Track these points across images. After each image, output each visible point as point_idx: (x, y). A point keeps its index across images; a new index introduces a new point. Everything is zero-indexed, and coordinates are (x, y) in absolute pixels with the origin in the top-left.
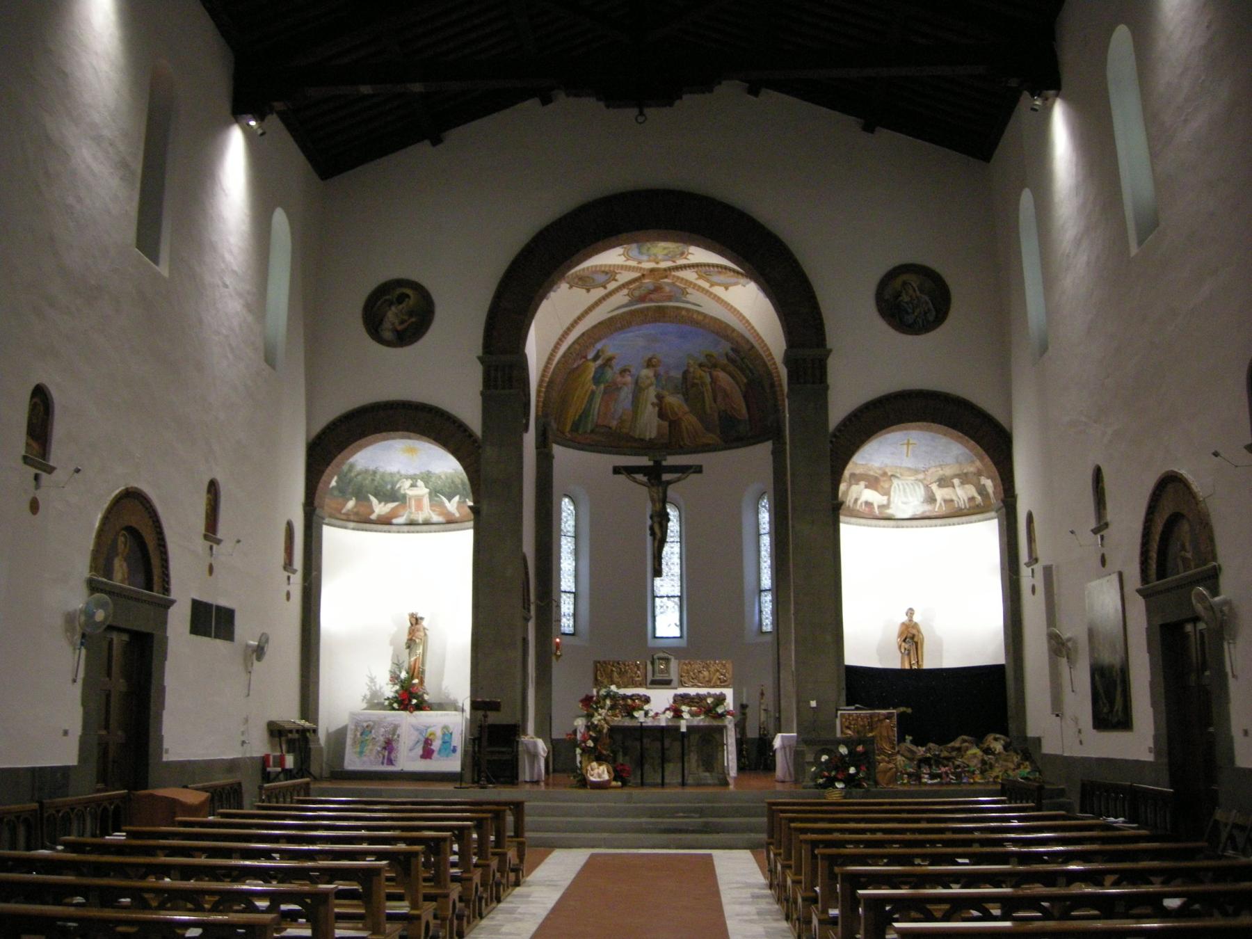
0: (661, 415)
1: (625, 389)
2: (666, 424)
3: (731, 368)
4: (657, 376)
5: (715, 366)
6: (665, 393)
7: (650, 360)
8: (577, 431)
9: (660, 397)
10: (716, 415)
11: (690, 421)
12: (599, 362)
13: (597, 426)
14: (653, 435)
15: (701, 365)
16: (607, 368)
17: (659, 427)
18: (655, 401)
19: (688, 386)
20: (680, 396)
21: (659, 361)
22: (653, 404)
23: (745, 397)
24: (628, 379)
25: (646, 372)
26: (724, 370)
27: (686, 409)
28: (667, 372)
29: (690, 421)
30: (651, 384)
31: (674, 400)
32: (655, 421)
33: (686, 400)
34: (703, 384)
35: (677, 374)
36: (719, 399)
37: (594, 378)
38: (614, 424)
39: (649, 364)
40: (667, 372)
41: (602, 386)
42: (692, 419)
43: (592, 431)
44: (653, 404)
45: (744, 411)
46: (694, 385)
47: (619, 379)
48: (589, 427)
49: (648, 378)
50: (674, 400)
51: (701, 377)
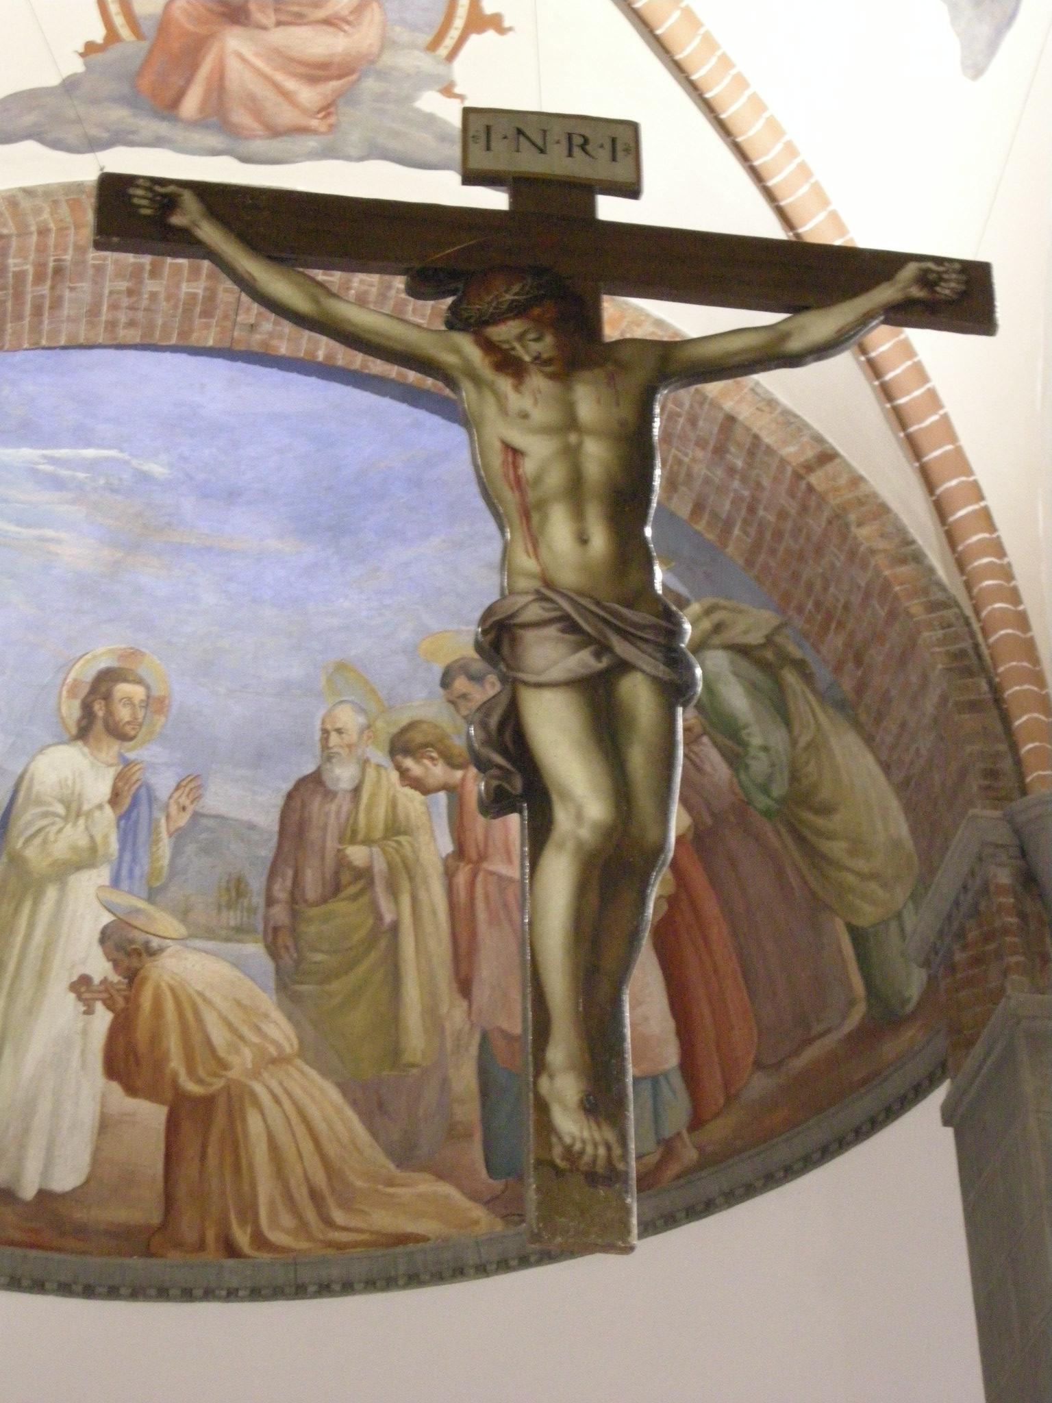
0: (126, 1061)
2: (152, 1114)
4: (128, 799)
6: (165, 924)
7: (105, 681)
9: (128, 950)
10: (465, 1078)
11: (299, 1107)
14: (66, 1179)
15: (402, 746)
17: (105, 1125)
18: (100, 968)
19: (305, 891)
20: (254, 950)
21: (155, 704)
22: (81, 986)
25: (73, 771)
27: (280, 1030)
28: (191, 784)
29: (299, 1107)
30: (87, 859)
31: (216, 978)
32: (88, 1090)
33: (289, 981)
34: (403, 872)
35: (249, 804)
39: (98, 712)
40: (191, 784)
42: (324, 1099)
44: (81, 986)
46: (346, 880)
49: (74, 809)
50: (216, 978)
51: (396, 828)
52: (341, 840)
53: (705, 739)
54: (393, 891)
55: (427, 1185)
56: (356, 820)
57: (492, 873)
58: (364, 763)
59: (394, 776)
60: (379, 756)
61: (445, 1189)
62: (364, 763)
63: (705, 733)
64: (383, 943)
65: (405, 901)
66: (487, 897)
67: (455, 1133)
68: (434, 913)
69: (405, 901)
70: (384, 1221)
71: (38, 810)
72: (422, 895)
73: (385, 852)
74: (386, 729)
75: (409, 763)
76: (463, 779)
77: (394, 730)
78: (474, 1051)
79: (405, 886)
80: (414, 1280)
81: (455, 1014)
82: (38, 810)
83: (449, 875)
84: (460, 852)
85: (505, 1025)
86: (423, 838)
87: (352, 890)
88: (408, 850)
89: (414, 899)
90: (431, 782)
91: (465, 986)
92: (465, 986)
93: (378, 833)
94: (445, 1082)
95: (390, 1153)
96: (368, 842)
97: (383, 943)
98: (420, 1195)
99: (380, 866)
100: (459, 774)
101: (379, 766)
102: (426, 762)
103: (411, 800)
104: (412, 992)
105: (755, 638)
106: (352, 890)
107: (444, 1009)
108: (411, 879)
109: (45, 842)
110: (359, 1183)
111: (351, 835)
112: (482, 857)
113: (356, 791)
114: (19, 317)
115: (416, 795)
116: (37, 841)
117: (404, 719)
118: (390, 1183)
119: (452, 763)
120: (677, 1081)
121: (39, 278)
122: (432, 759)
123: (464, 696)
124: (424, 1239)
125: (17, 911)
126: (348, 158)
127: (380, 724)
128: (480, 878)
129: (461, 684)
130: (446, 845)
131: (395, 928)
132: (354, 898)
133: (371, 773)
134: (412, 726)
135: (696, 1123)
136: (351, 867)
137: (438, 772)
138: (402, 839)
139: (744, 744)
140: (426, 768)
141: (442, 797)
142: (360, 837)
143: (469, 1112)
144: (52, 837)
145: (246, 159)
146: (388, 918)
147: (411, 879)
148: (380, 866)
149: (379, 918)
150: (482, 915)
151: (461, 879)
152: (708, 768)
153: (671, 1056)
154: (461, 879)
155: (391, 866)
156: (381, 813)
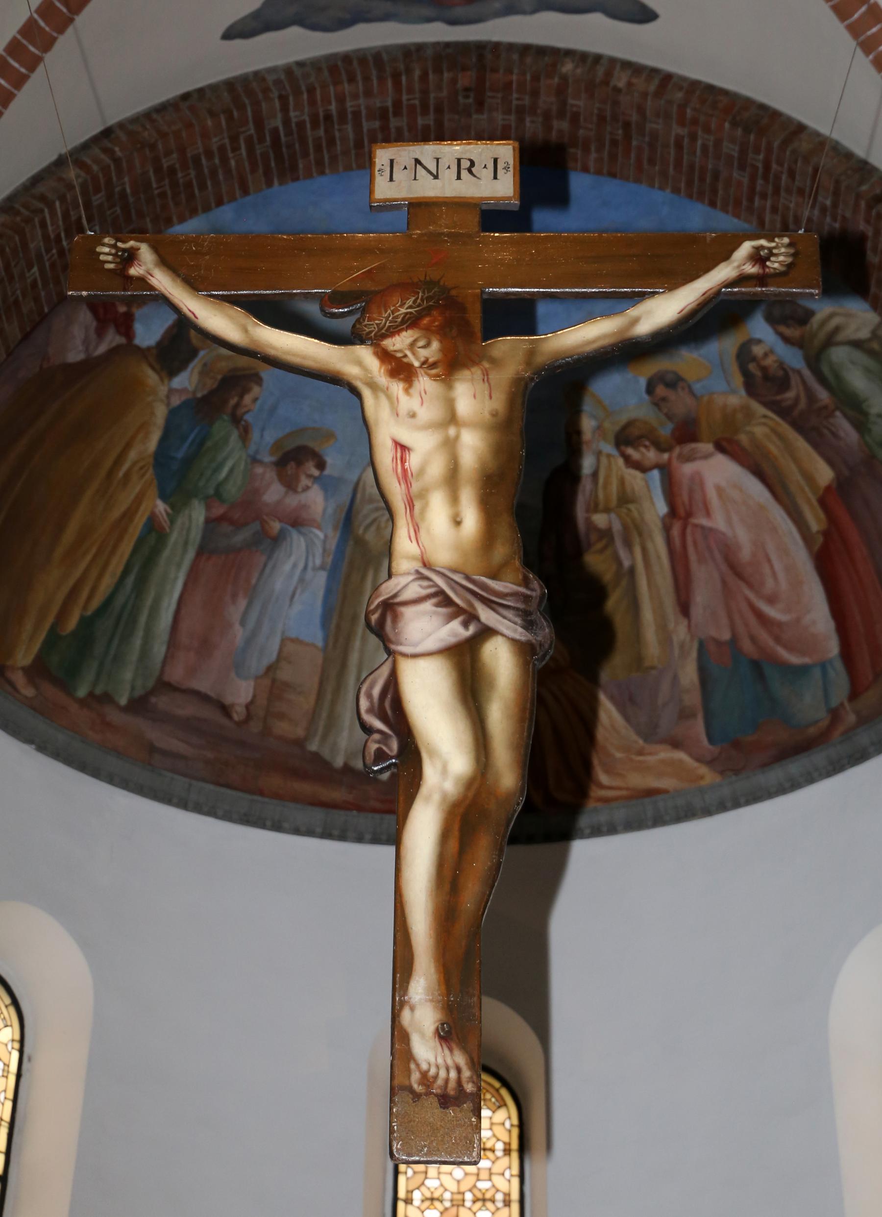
1: (297, 542)
3: (763, 427)
5: (687, 433)
8: (65, 684)
10: (689, 674)
12: (186, 381)
13: (164, 686)
16: (222, 427)
23: (827, 561)
24: (315, 500)
26: (725, 446)
34: (634, 530)
36: (703, 595)
37: (161, 458)
38: (241, 693)
41: (198, 514)
43: (139, 705)
45: (819, 618)
47: (273, 492)
48: (127, 683)
51: (626, 499)
52: (588, 511)
53: (838, 413)
54: (628, 544)
55: (665, 754)
56: (596, 496)
57: (696, 526)
58: (599, 454)
59: (621, 461)
60: (608, 448)
61: (681, 755)
62: (599, 454)
63: (837, 408)
64: (624, 582)
65: (638, 551)
66: (695, 543)
67: (685, 715)
68: (659, 557)
69: (638, 551)
70: (638, 781)
71: (371, 506)
72: (649, 545)
73: (620, 517)
74: (612, 427)
75: (630, 451)
76: (670, 459)
77: (617, 428)
78: (694, 654)
79: (636, 540)
80: (658, 821)
81: (680, 631)
82: (371, 506)
83: (667, 529)
84: (673, 512)
85: (713, 633)
86: (646, 505)
87: (599, 546)
88: (635, 514)
89: (644, 551)
90: (647, 463)
91: (684, 608)
92: (684, 608)
93: (614, 502)
94: (675, 679)
95: (639, 733)
96: (607, 510)
97: (624, 582)
98: (663, 761)
99: (617, 527)
100: (666, 456)
101: (609, 456)
102: (643, 449)
103: (635, 478)
104: (648, 615)
105: (864, 334)
106: (599, 546)
107: (671, 626)
108: (640, 534)
109: (379, 528)
110: (619, 755)
111: (594, 507)
112: (689, 514)
113: (595, 475)
114: (306, 154)
115: (637, 474)
116: (373, 528)
117: (624, 419)
118: (641, 753)
119: (661, 447)
120: (839, 665)
121: (315, 124)
122: (646, 447)
123: (664, 399)
124: (664, 791)
125: (363, 579)
126: (524, 12)
127: (607, 425)
128: (689, 530)
129: (661, 390)
130: (662, 508)
131: (632, 571)
132: (602, 551)
133: (604, 461)
134: (629, 424)
135: (854, 695)
136: (599, 530)
137: (651, 455)
138: (632, 506)
139: (866, 414)
140: (643, 454)
141: (656, 473)
142: (601, 506)
143: (693, 699)
144: (383, 525)
145: (453, 22)
146: (627, 563)
147: (640, 534)
148: (617, 527)
149: (619, 563)
150: (693, 557)
151: (676, 532)
152: (842, 434)
153: (833, 648)
154: (676, 532)
155: (625, 527)
156: (614, 488)
